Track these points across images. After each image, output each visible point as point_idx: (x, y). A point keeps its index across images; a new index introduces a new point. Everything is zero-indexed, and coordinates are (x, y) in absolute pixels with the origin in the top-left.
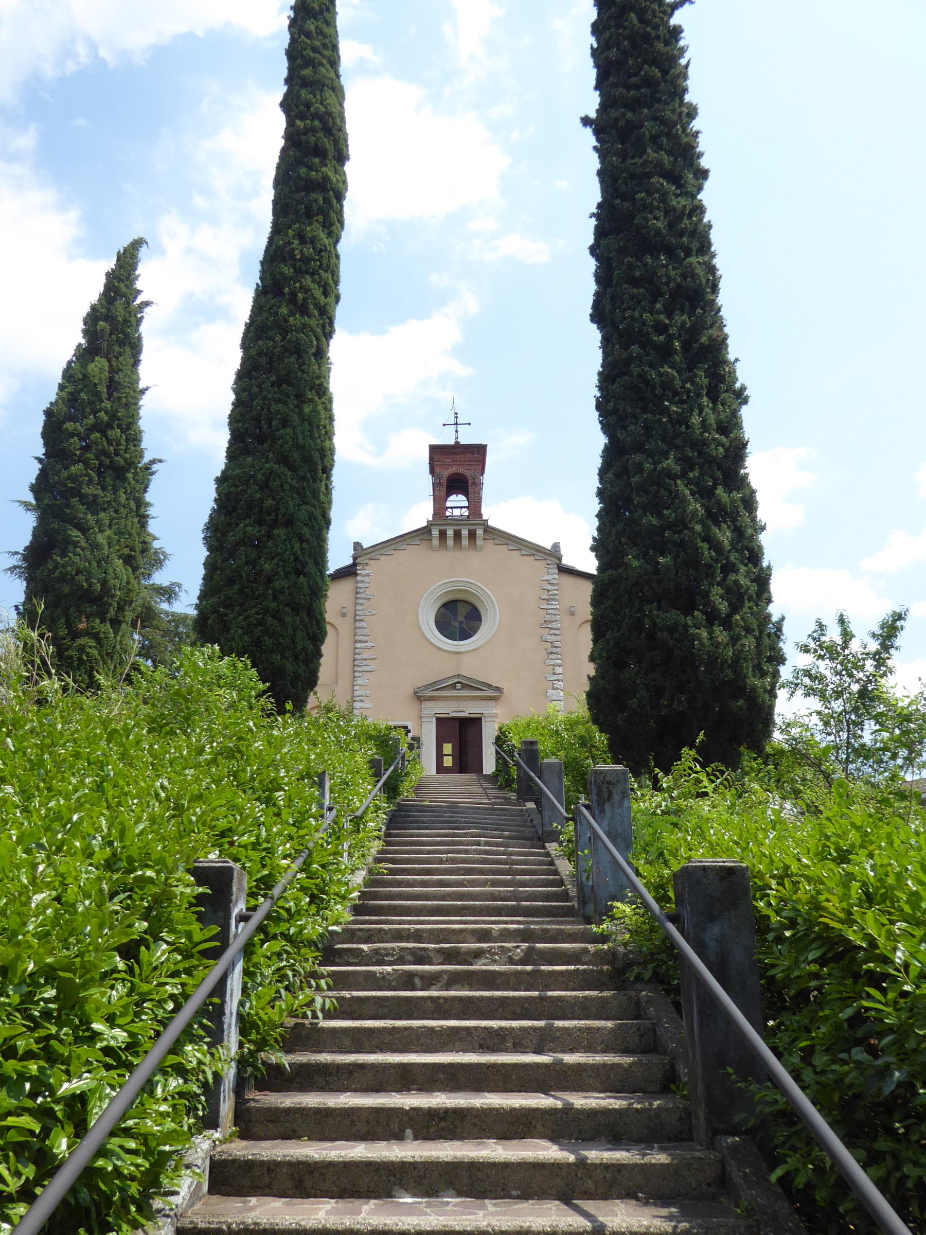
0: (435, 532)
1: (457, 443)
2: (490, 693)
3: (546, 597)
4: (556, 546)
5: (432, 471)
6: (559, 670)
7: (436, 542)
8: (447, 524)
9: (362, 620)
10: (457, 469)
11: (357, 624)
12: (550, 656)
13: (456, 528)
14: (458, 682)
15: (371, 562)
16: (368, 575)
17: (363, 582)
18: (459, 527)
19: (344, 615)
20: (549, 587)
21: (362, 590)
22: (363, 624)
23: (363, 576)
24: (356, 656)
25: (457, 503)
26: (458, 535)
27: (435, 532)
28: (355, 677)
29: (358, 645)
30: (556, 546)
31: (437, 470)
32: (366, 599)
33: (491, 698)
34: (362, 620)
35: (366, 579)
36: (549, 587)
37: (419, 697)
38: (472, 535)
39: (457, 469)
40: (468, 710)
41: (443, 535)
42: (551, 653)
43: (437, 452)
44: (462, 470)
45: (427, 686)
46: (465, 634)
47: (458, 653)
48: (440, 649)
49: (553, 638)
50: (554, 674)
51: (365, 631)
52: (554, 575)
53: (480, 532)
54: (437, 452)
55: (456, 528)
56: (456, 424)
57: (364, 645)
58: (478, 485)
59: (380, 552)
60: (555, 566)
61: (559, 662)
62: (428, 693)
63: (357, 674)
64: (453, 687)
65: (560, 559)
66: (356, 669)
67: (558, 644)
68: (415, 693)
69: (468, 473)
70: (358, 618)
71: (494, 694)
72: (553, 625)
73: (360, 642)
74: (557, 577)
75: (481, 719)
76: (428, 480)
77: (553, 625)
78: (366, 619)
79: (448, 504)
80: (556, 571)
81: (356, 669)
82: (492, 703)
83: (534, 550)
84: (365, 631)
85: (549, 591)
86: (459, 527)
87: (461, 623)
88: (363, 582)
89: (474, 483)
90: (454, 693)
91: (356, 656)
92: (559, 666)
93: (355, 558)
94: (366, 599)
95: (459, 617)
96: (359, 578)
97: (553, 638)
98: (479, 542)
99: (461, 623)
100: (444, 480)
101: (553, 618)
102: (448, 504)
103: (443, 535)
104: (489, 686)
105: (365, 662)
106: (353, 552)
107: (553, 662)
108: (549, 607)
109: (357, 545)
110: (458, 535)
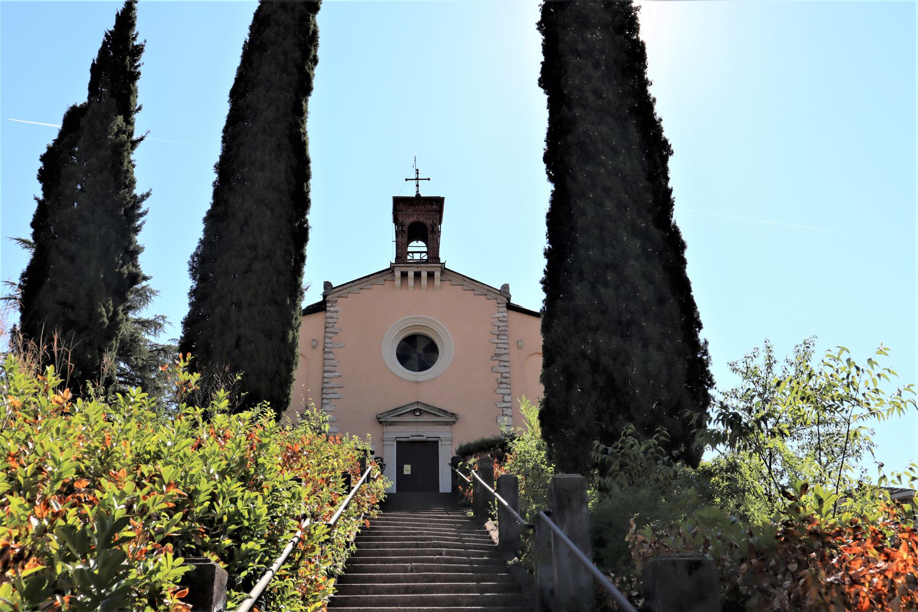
0: (398, 274)
1: (418, 195)
2: (446, 419)
3: (497, 333)
4: (506, 287)
5: (396, 220)
6: (507, 398)
7: (398, 282)
9: (331, 352)
10: (418, 218)
11: (326, 356)
12: (501, 386)
14: (416, 410)
15: (339, 300)
16: (336, 312)
17: (332, 318)
19: (314, 347)
20: (500, 324)
21: (331, 325)
22: (331, 356)
23: (332, 312)
24: (325, 385)
25: (417, 247)
26: (418, 275)
28: (323, 404)
29: (326, 375)
30: (506, 287)
31: (400, 219)
32: (334, 333)
33: (446, 423)
34: (331, 352)
35: (334, 315)
36: (500, 324)
37: (382, 421)
38: (431, 275)
39: (418, 218)
40: (428, 433)
41: (404, 275)
42: (501, 383)
43: (399, 203)
44: (421, 220)
45: (389, 412)
46: (424, 366)
47: (417, 382)
48: (400, 378)
49: (503, 370)
50: (504, 402)
51: (333, 362)
52: (504, 313)
53: (437, 274)
54: (399, 203)
55: (416, 270)
56: (417, 179)
57: (332, 375)
58: (437, 233)
61: (508, 391)
62: (390, 419)
63: (325, 401)
64: (414, 411)
65: (509, 299)
66: (324, 396)
67: (507, 375)
68: (378, 418)
69: (428, 222)
70: (326, 350)
71: (451, 419)
72: (502, 358)
73: (328, 371)
74: (505, 314)
75: (437, 442)
76: (392, 228)
77: (502, 358)
78: (334, 351)
79: (409, 249)
81: (324, 396)
82: (448, 428)
83: (487, 290)
84: (333, 362)
86: (419, 269)
87: (420, 356)
88: (332, 318)
89: (433, 231)
90: (414, 419)
91: (325, 385)
92: (509, 395)
93: (325, 296)
94: (334, 333)
95: (417, 351)
96: (328, 314)
97: (503, 370)
98: (437, 282)
99: (420, 356)
100: (405, 228)
101: (503, 351)
102: (409, 249)
103: (404, 275)
104: (446, 412)
105: (332, 391)
107: (502, 391)
109: (327, 285)
110: (418, 275)
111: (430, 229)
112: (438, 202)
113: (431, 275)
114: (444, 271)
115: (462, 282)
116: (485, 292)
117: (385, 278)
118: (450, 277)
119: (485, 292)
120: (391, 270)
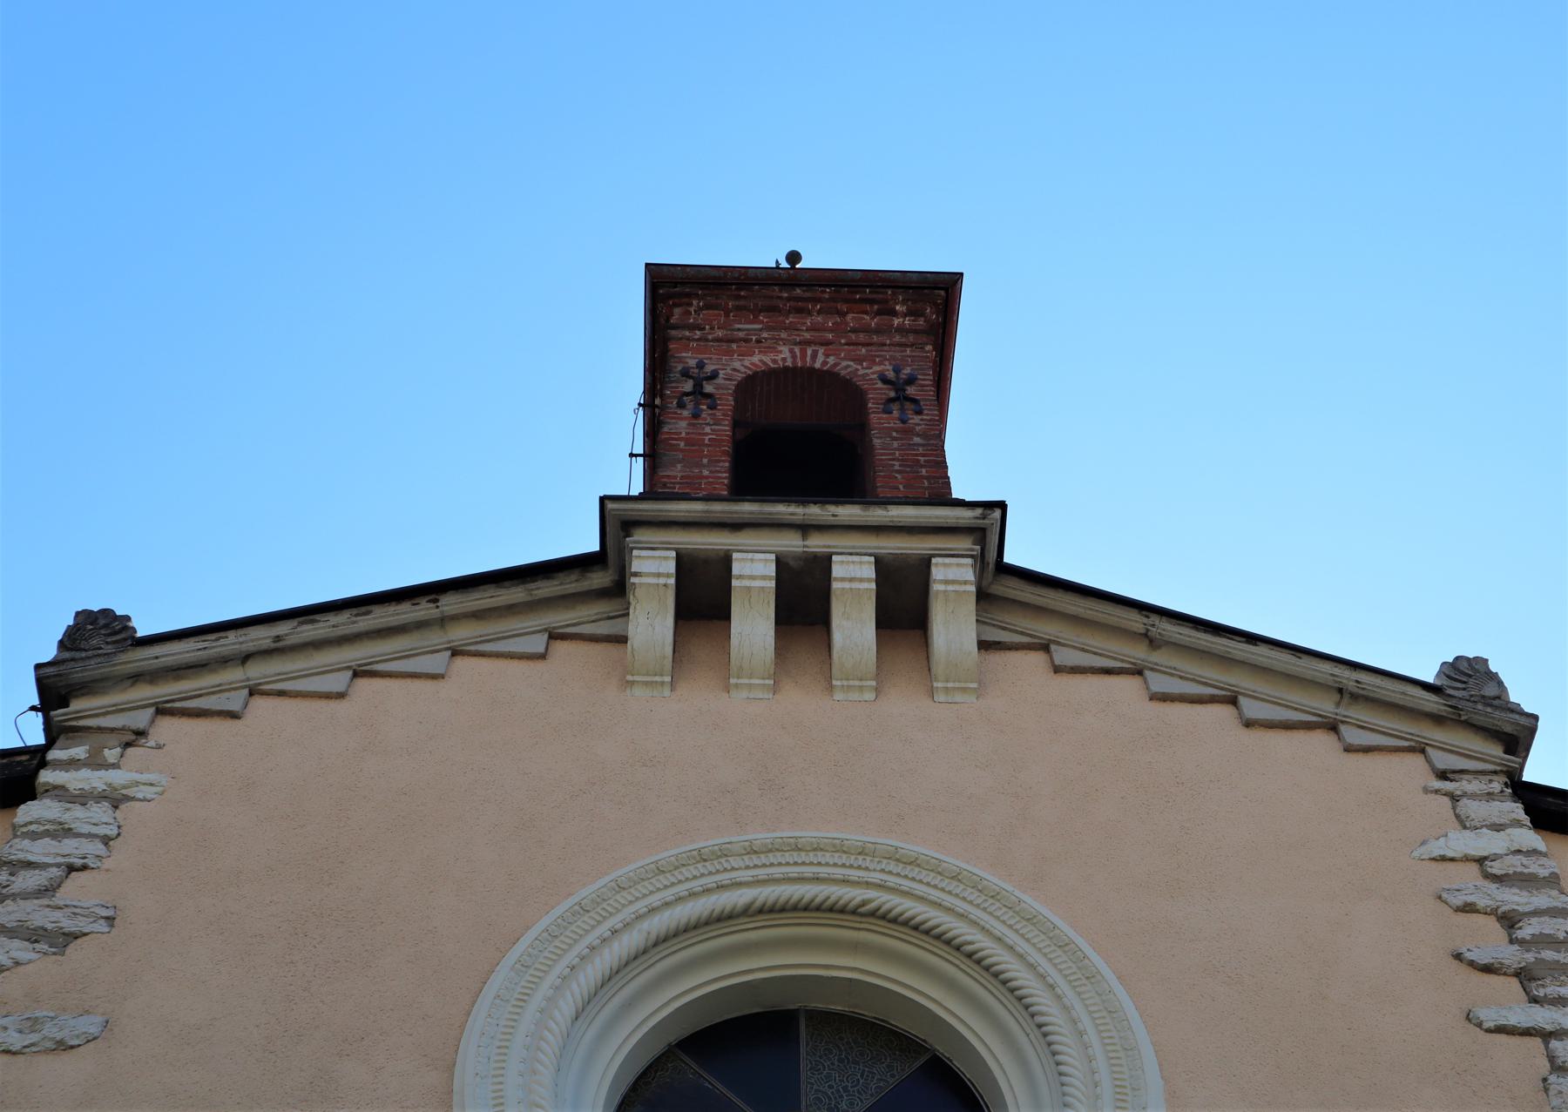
0: (653, 566)
7: (652, 622)
8: (736, 526)
10: (800, 408)
13: (791, 543)
18: (818, 543)
20: (1513, 898)
27: (653, 566)
36: (1513, 898)
38: (903, 609)
39: (800, 408)
41: (703, 599)
53: (953, 575)
55: (791, 543)
59: (257, 671)
60: (1497, 786)
65: (1517, 735)
69: (868, 372)
74: (1531, 839)
80: (1518, 810)
83: (1340, 696)
85: (1509, 921)
86: (818, 543)
89: (901, 398)
98: (953, 626)
100: (723, 388)
106: (49, 653)
108: (1543, 1017)
111: (877, 394)
112: (932, 301)
113: (903, 609)
114: (1007, 589)
115: (1137, 653)
116: (1326, 705)
117: (559, 618)
118: (1046, 629)
119: (1326, 705)
120: (597, 576)
